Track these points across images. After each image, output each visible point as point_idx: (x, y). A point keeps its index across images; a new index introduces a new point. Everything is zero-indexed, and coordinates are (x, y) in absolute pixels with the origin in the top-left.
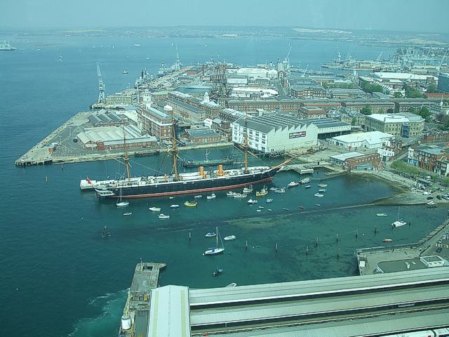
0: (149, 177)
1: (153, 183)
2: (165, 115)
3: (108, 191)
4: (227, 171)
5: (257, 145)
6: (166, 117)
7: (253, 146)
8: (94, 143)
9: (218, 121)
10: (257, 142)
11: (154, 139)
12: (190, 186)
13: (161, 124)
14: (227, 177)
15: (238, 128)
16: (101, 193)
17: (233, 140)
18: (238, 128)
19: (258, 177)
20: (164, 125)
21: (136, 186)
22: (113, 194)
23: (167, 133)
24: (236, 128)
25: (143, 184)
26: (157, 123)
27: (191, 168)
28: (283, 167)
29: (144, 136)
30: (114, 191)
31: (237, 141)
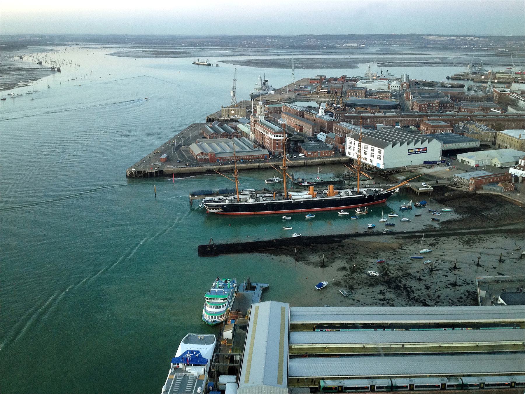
0: (258, 195)
1: (262, 201)
2: (277, 128)
3: (216, 208)
4: (338, 191)
5: (372, 161)
6: (279, 130)
7: (368, 162)
8: (206, 155)
9: (333, 135)
10: (372, 158)
11: (266, 152)
12: (299, 205)
13: (273, 137)
14: (338, 197)
15: (353, 143)
16: (210, 209)
17: (347, 155)
18: (353, 143)
19: (370, 198)
20: (276, 138)
21: (246, 203)
22: (221, 210)
23: (279, 147)
24: (350, 143)
25: (251, 201)
26: (270, 136)
27: (298, 186)
28: (398, 189)
29: (256, 149)
30: (222, 206)
31: (351, 156)
